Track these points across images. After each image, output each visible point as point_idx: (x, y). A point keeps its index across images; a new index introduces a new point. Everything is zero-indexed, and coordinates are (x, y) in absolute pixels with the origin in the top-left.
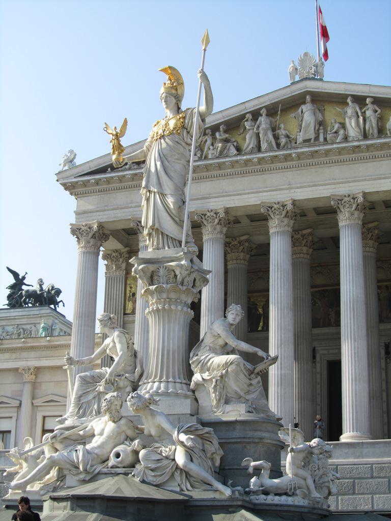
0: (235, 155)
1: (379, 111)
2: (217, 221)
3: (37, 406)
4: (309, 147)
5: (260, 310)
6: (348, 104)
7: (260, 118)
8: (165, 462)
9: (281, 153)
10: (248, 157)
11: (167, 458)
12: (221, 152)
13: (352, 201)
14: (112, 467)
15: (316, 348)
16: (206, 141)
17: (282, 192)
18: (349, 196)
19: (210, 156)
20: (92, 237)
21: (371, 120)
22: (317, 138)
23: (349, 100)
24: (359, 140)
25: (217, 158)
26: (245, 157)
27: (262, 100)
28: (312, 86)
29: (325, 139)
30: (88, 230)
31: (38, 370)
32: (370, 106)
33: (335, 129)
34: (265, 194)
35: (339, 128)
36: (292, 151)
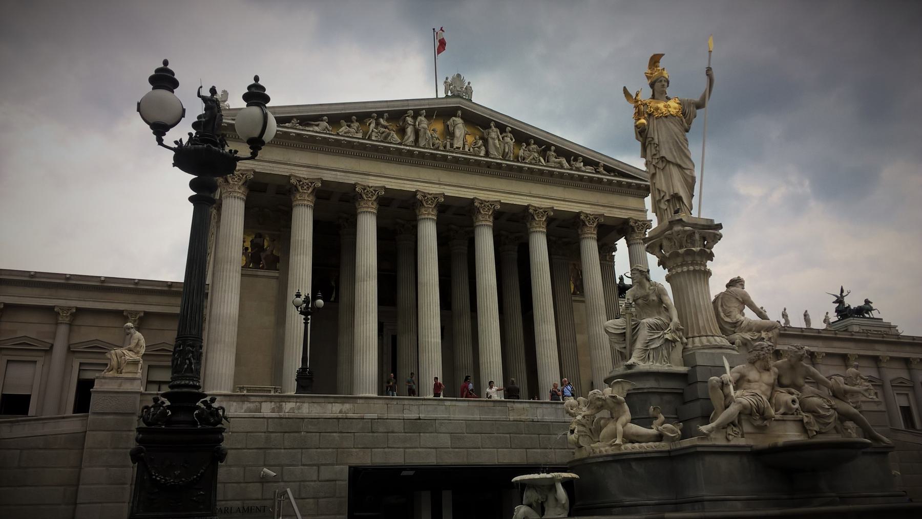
0: (400, 144)
1: (514, 140)
2: (374, 197)
3: (74, 352)
4: (462, 154)
5: (333, 284)
6: (491, 127)
7: (419, 118)
8: (832, 412)
9: (439, 152)
10: (411, 148)
11: (832, 407)
12: (386, 138)
13: (490, 206)
14: (784, 414)
15: (384, 324)
16: (370, 124)
17: (433, 186)
18: (488, 201)
19: (373, 138)
20: (243, 184)
21: (509, 147)
22: (464, 148)
23: (492, 125)
24: (500, 159)
25: (382, 141)
26: (408, 148)
27: (423, 102)
28: (464, 105)
29: (469, 150)
30: (241, 175)
31: (80, 310)
32: (509, 135)
33: (479, 145)
34: (419, 184)
35: (481, 145)
36: (448, 154)
